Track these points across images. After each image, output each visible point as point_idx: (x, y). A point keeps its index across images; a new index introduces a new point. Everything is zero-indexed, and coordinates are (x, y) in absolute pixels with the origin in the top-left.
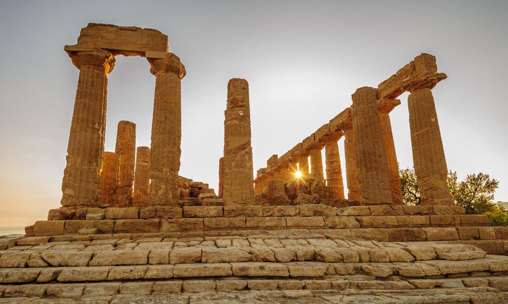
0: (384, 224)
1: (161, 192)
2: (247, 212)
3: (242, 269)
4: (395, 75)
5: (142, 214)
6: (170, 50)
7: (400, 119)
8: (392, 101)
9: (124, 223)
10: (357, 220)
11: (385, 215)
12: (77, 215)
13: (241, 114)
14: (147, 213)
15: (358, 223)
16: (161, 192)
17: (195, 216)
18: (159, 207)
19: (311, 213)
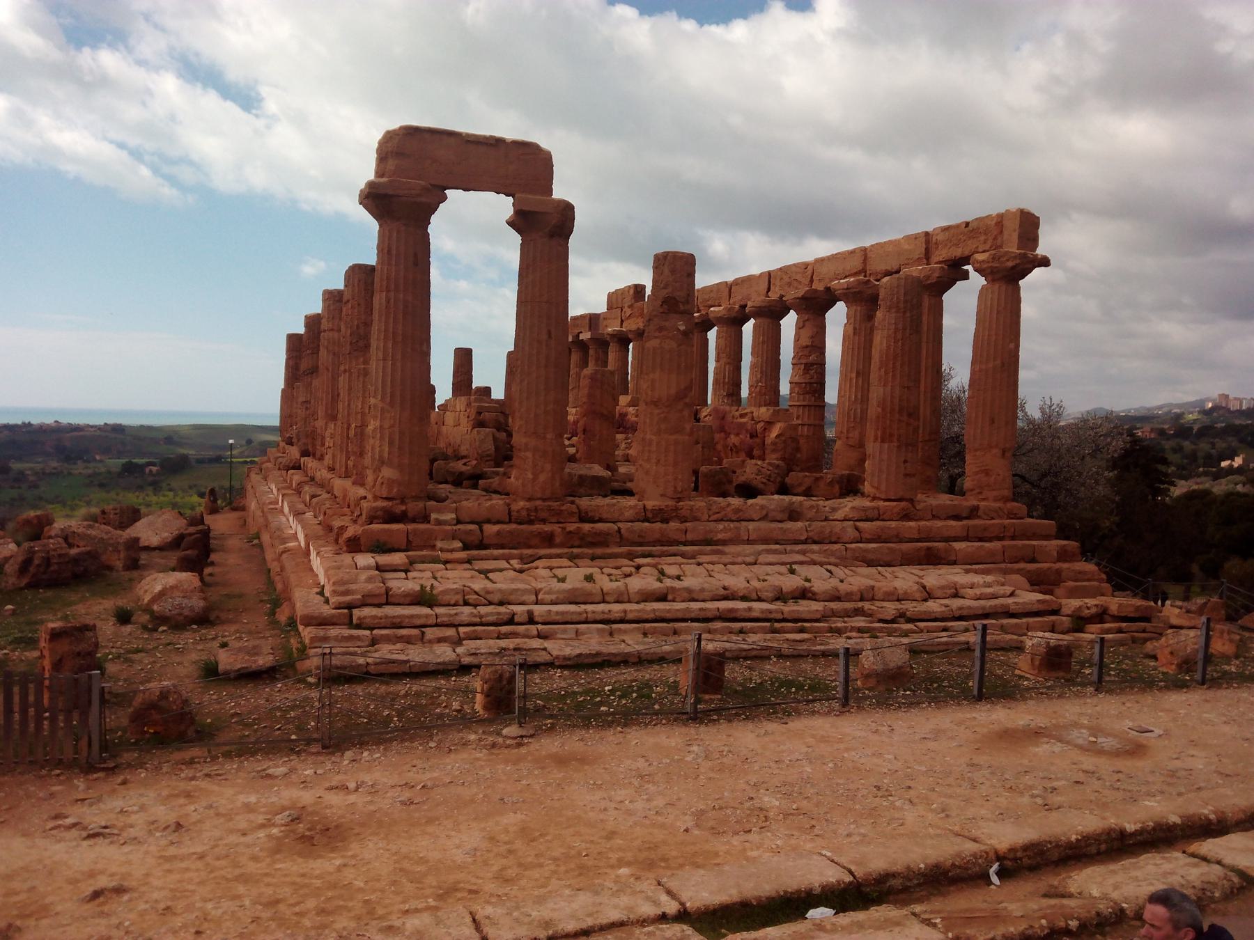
0: (897, 536)
1: (542, 478)
2: (683, 513)
3: (732, 610)
4: (967, 224)
5: (514, 514)
6: (559, 192)
7: (962, 306)
8: (954, 272)
9: (498, 533)
10: (857, 529)
11: (902, 519)
12: (410, 515)
13: (682, 328)
14: (524, 513)
15: (857, 534)
16: (542, 478)
17: (601, 520)
18: (538, 503)
19: (785, 516)
